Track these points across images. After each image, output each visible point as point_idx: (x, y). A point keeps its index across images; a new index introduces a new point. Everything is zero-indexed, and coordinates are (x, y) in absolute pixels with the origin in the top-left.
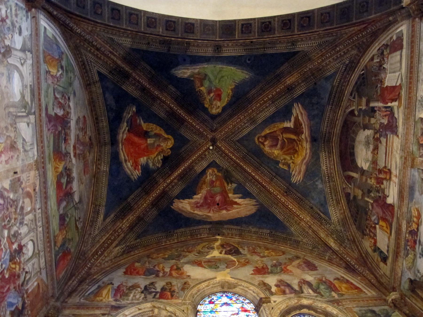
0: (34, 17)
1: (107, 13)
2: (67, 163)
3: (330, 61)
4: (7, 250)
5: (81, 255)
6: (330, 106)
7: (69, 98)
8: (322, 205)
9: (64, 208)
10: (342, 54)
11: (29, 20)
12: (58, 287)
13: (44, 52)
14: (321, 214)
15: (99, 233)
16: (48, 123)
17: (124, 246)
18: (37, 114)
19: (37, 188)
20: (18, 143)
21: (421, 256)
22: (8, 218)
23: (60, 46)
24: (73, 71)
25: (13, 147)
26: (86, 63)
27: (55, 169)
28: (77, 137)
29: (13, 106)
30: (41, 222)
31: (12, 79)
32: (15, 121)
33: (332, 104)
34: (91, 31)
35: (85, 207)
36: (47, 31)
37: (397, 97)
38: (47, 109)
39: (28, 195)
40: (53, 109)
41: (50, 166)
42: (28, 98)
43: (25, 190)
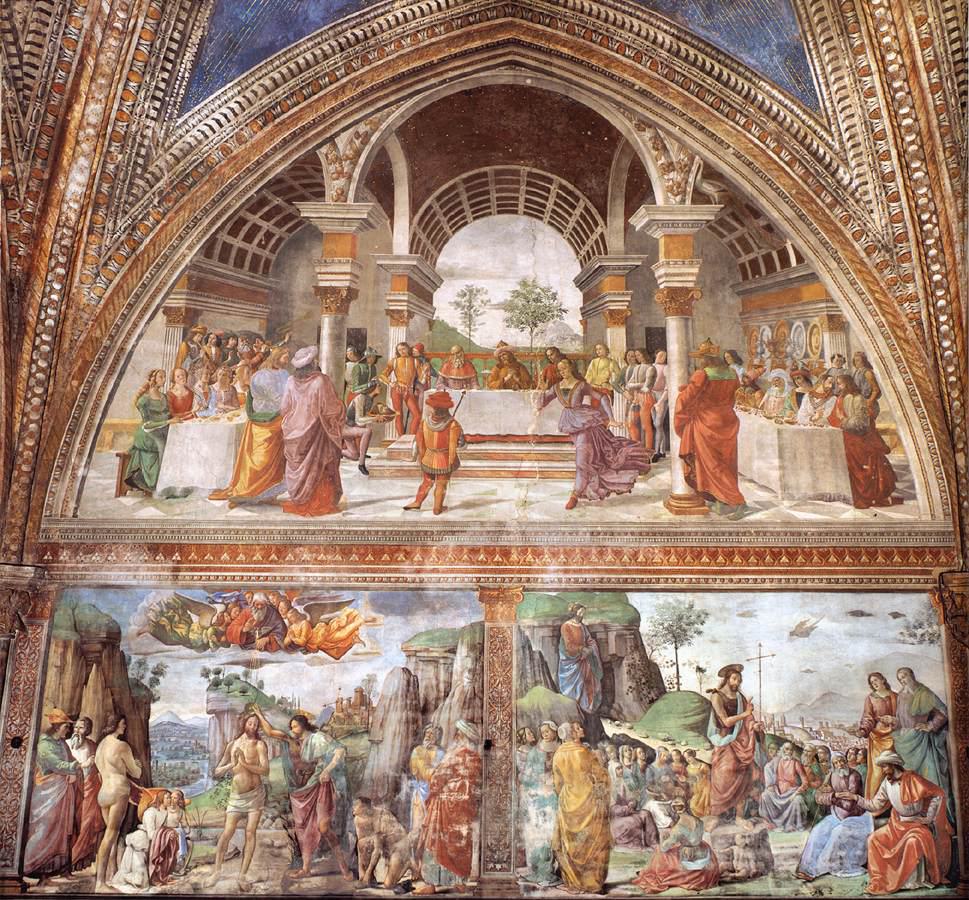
3: (871, 93)
6: (668, 39)
8: (231, 45)
10: (887, 167)
14: (189, 56)
21: (212, 677)
33: (677, 54)
37: (700, 488)
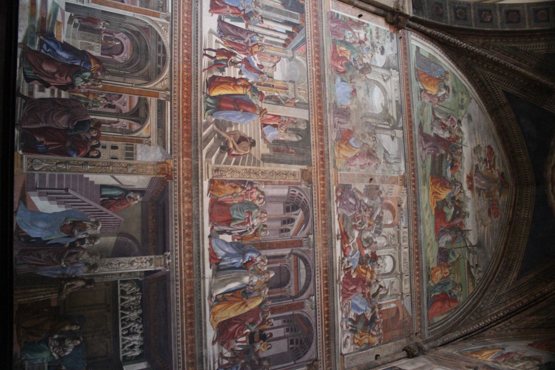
0: (401, 38)
1: (499, 18)
2: (456, 193)
4: (356, 251)
5: (476, 311)
7: (459, 122)
9: (447, 242)
11: (395, 40)
12: (429, 330)
13: (416, 70)
15: (507, 292)
16: (423, 142)
17: (544, 317)
18: (405, 129)
19: (404, 205)
20: (377, 152)
22: (360, 221)
23: (443, 66)
24: (467, 92)
25: (370, 154)
26: (486, 83)
27: (433, 193)
28: (475, 168)
29: (373, 116)
30: (407, 243)
31: (372, 93)
32: (374, 131)
34: (483, 44)
35: (490, 256)
36: (421, 50)
38: (421, 127)
39: (389, 207)
40: (432, 129)
41: (426, 187)
42: (393, 112)
43: (385, 201)
